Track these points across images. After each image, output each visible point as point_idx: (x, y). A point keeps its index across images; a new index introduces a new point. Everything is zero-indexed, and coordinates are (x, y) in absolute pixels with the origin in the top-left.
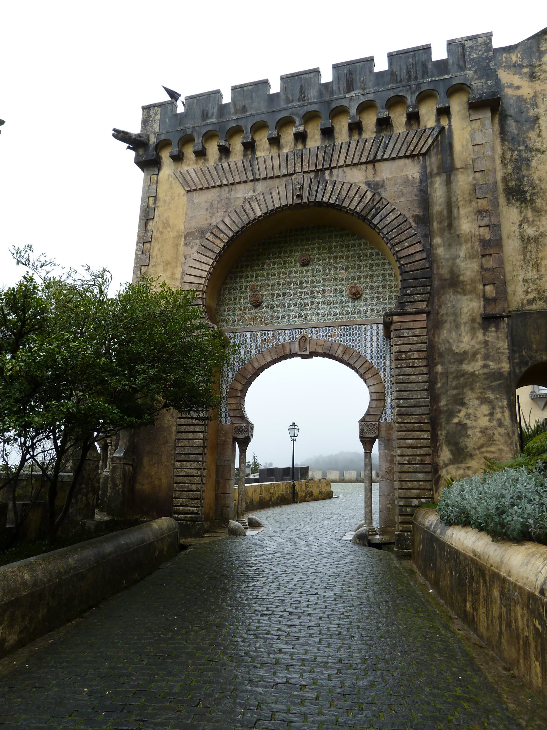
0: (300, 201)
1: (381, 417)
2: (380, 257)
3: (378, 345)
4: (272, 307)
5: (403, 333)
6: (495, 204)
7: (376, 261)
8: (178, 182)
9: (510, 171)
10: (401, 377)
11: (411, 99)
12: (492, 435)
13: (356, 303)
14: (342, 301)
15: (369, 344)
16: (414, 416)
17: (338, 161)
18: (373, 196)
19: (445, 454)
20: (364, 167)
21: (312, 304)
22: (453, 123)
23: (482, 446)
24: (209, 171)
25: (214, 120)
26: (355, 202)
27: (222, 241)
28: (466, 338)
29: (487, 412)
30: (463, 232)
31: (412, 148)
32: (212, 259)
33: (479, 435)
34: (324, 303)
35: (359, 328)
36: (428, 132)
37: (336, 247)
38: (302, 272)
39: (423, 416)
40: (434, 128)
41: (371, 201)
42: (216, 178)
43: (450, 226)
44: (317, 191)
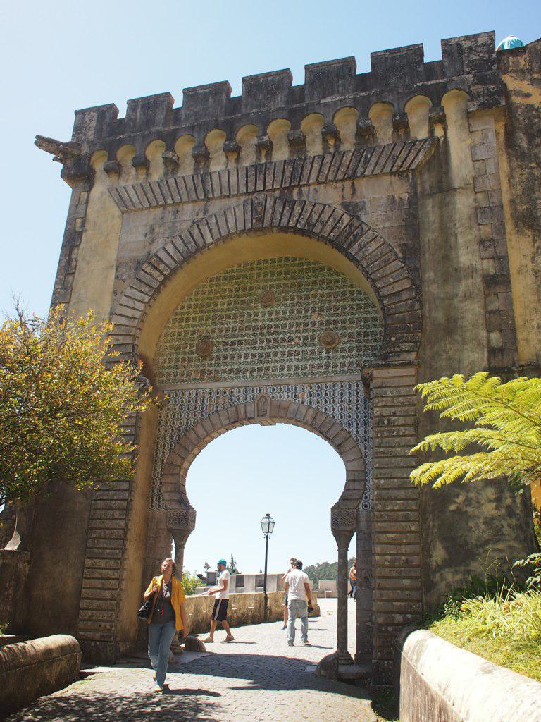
0: (261, 226)
1: (360, 502)
2: (362, 296)
3: (357, 409)
4: (225, 358)
5: (385, 392)
6: (501, 230)
7: (357, 302)
8: (112, 201)
9: (519, 192)
11: (398, 105)
12: (500, 526)
13: (331, 354)
14: (313, 352)
15: (346, 406)
16: (398, 502)
17: (309, 178)
18: (350, 221)
19: (439, 554)
20: (340, 185)
21: (275, 355)
22: (449, 135)
23: (487, 542)
24: (151, 189)
25: (160, 128)
26: (328, 228)
27: (162, 273)
29: (492, 497)
30: (462, 265)
31: (399, 162)
32: (149, 296)
33: (483, 527)
34: (290, 354)
35: (334, 386)
36: (418, 145)
37: (307, 284)
38: (264, 314)
39: (410, 502)
40: (426, 140)
41: (348, 226)
42: (159, 196)
43: (446, 258)
44: (282, 214)
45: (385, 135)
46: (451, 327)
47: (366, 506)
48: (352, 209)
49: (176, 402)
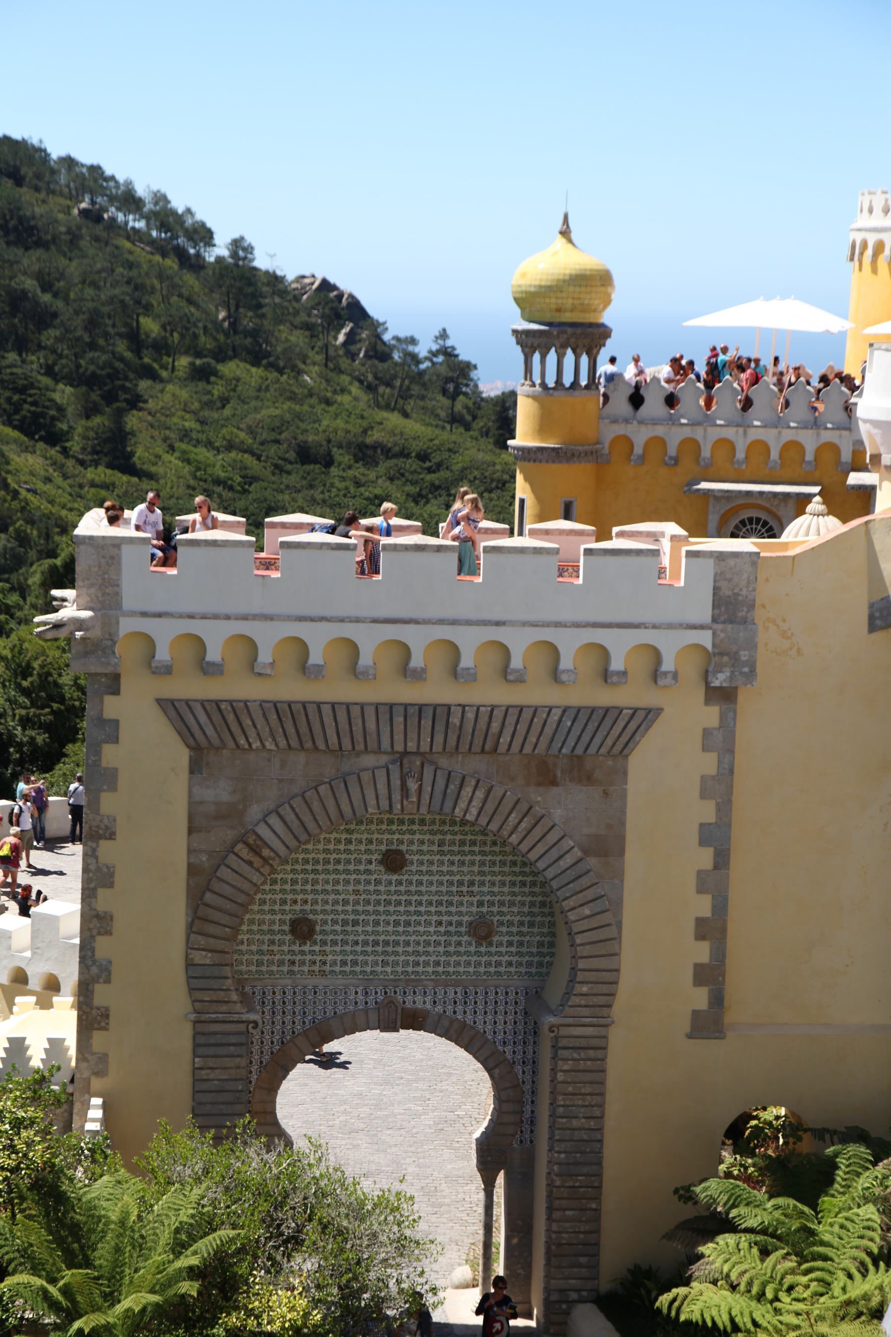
3: (515, 1023)
10: (564, 1120)
13: (483, 949)
15: (500, 1018)
34: (427, 943)
37: (452, 843)
47: (521, 1141)
49: (263, 1003)
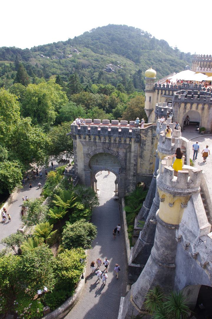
6: (137, 159)
19: (126, 192)
28: (131, 178)
43: (130, 161)
45: (123, 142)
46: (129, 169)
48: (118, 152)
